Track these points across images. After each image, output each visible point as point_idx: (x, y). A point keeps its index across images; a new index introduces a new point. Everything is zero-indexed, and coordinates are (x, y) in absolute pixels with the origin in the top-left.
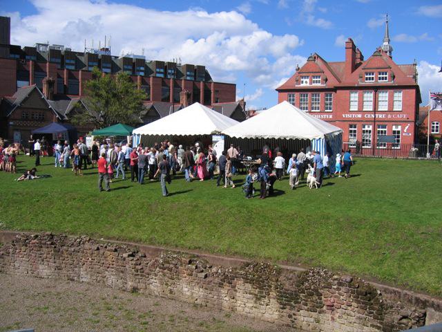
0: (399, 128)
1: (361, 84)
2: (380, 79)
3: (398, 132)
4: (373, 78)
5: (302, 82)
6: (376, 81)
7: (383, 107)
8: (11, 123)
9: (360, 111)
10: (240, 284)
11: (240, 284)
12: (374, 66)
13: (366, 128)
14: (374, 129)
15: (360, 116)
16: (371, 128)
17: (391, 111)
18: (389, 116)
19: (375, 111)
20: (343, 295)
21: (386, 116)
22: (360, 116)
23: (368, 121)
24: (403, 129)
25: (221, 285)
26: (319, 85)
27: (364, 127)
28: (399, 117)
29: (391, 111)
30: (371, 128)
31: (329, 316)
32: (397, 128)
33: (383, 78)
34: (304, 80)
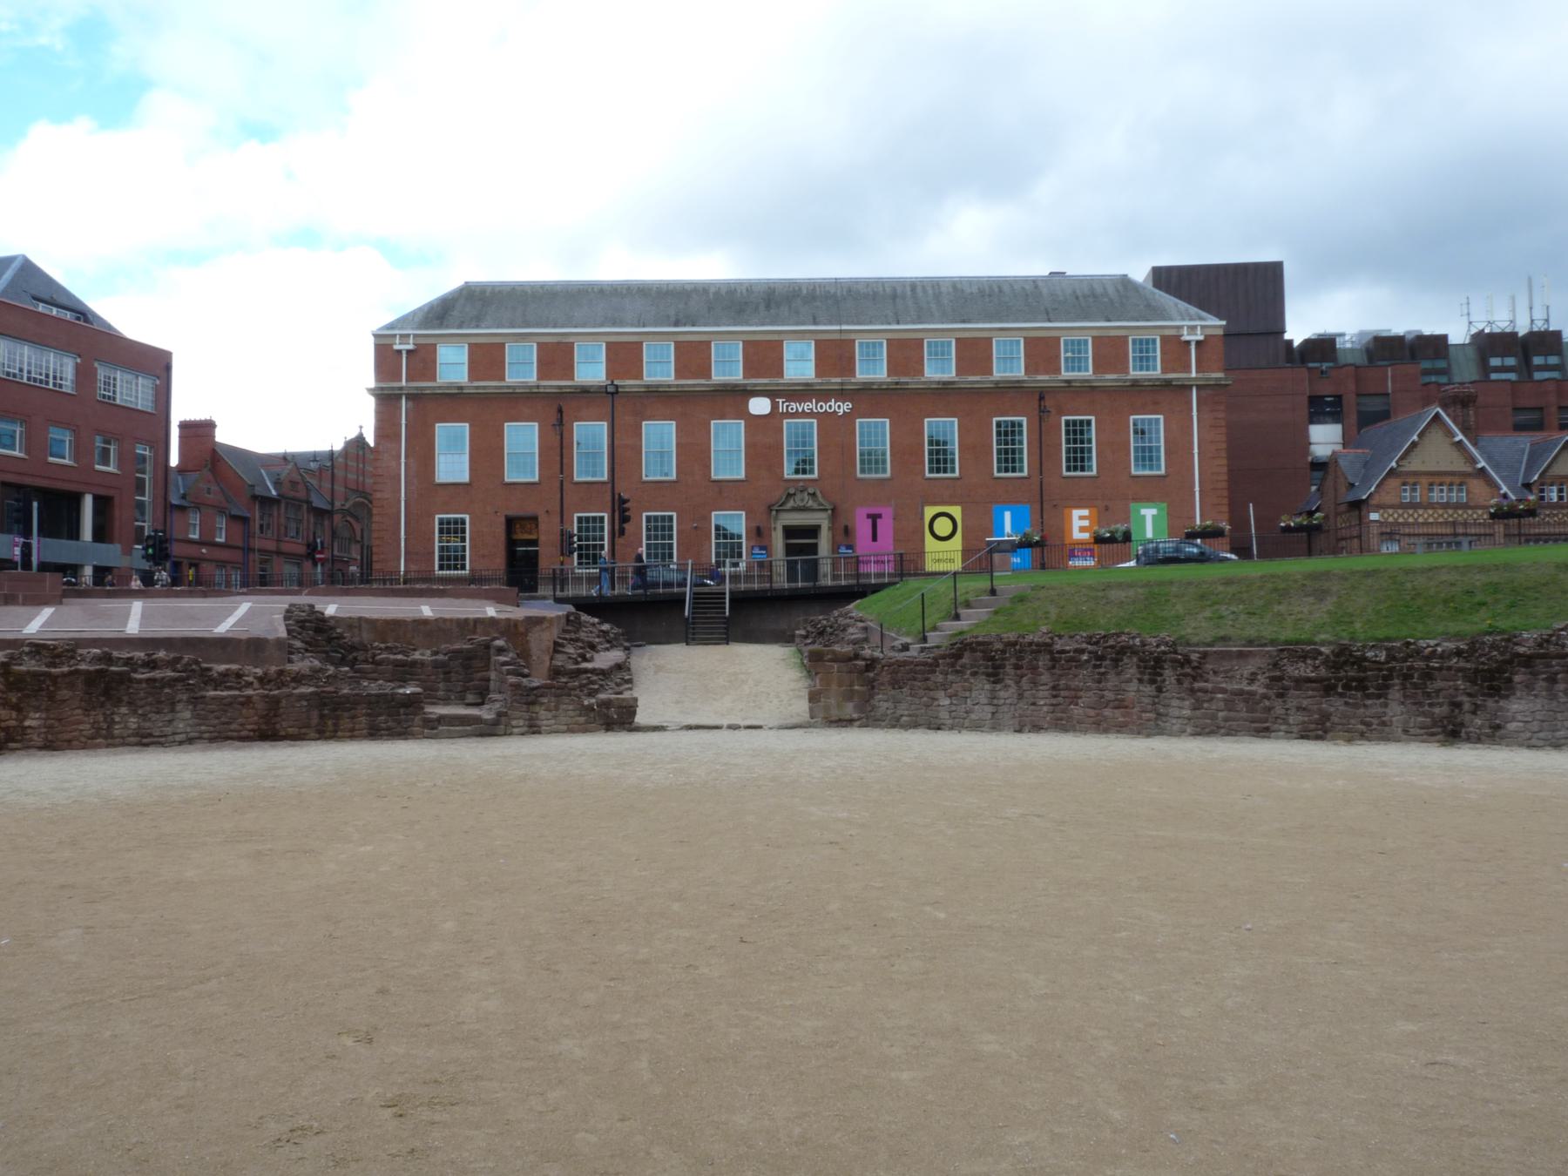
8: (1374, 516)
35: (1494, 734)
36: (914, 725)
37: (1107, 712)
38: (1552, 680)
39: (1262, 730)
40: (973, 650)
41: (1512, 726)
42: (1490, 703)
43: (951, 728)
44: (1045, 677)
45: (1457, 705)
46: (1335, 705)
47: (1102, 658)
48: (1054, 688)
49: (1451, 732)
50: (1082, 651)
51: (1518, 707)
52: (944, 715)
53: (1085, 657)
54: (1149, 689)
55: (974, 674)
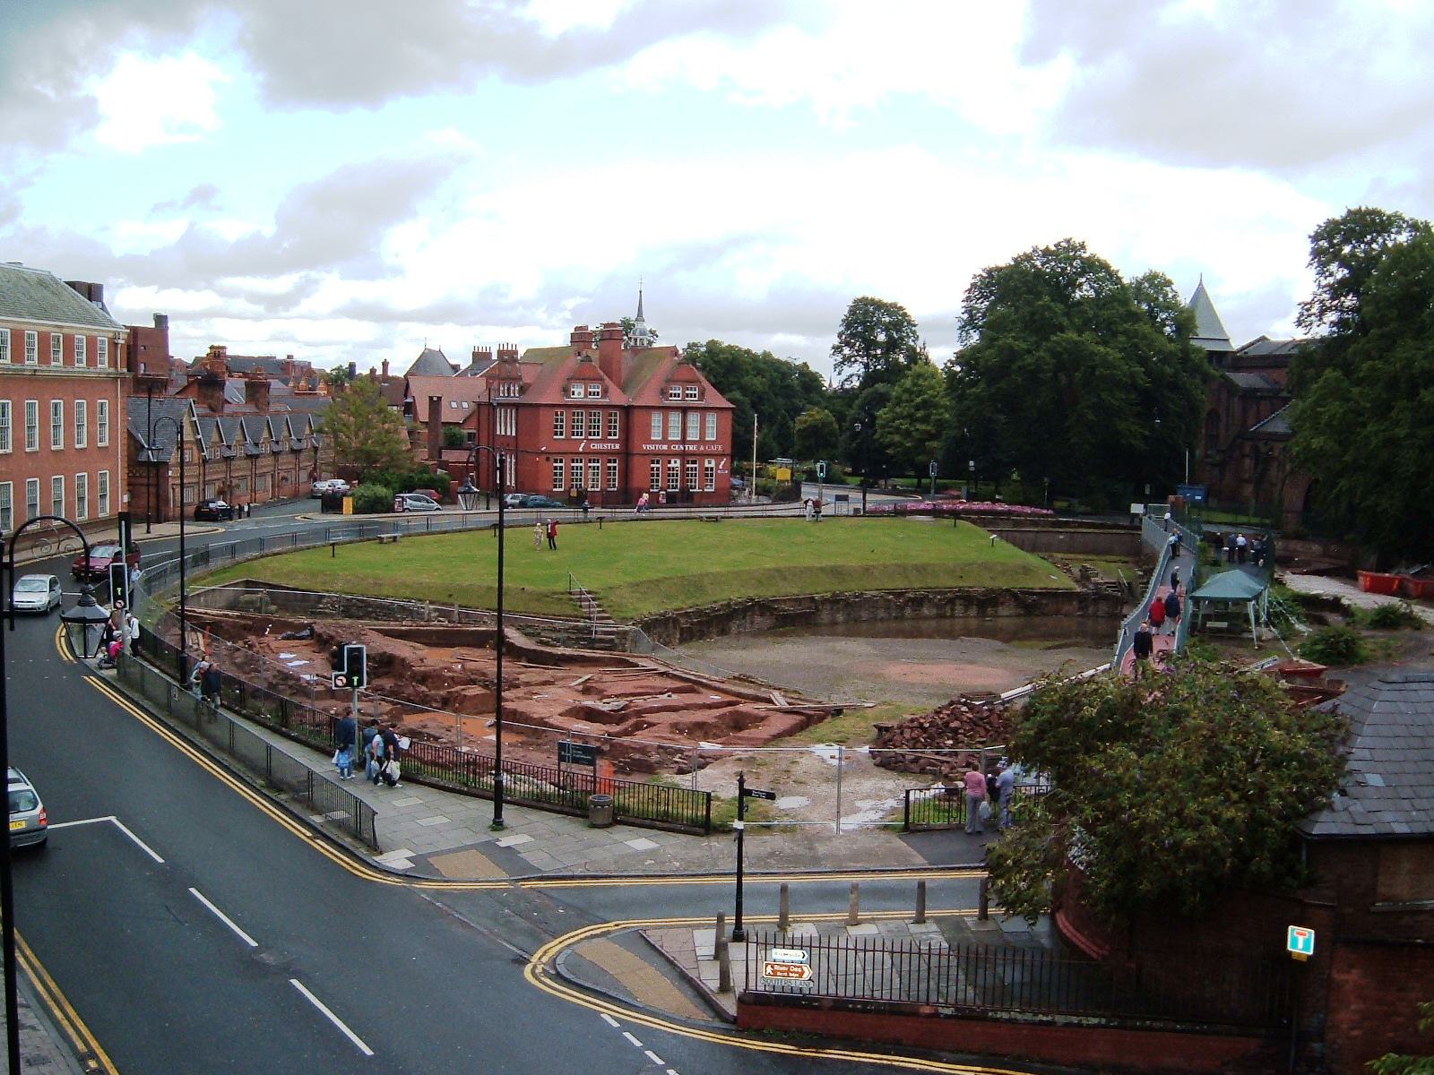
0: (713, 465)
1: (667, 403)
7: (693, 435)
9: (665, 441)
10: (958, 602)
11: (958, 602)
14: (683, 465)
15: (665, 447)
16: (678, 464)
17: (702, 441)
18: (702, 448)
19: (684, 441)
21: (698, 448)
22: (665, 447)
23: (675, 455)
24: (717, 465)
27: (670, 463)
28: (714, 448)
29: (702, 441)
32: (710, 463)
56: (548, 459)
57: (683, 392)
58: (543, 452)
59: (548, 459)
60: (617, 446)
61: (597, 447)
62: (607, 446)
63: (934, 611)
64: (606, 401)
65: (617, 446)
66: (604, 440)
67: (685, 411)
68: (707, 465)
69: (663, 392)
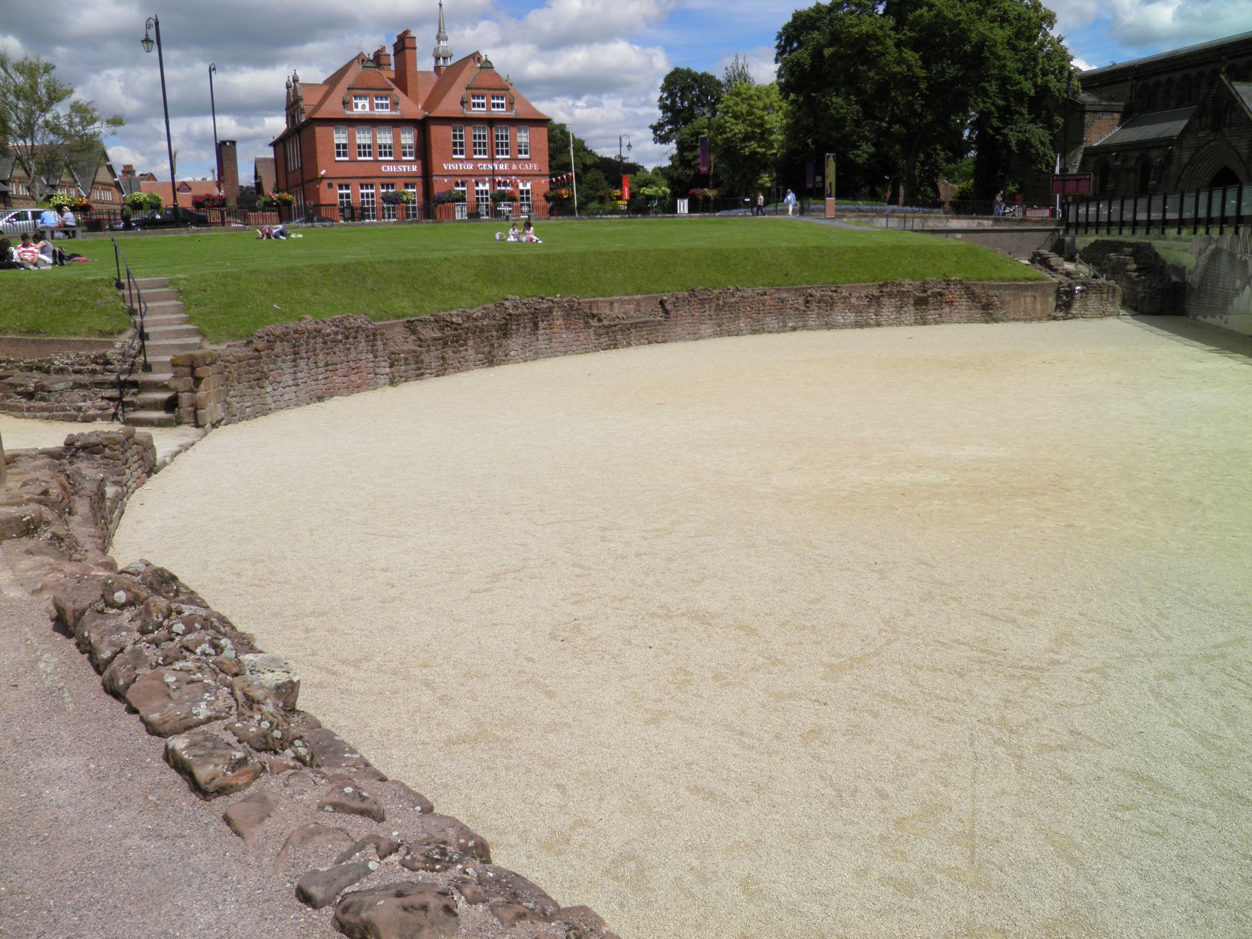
2: (494, 105)
3: (528, 192)
4: (483, 105)
5: (356, 106)
6: (488, 110)
10: (885, 300)
11: (885, 300)
12: (483, 84)
13: (481, 187)
14: (493, 187)
15: (470, 167)
16: (487, 187)
18: (514, 167)
20: (955, 293)
21: (510, 167)
22: (470, 167)
25: (869, 306)
26: (386, 113)
28: (528, 167)
30: (487, 187)
31: (947, 310)
32: (525, 185)
33: (498, 106)
34: (360, 103)
35: (506, 359)
36: (255, 415)
37: (353, 378)
38: (525, 327)
39: (420, 376)
40: (282, 341)
41: (513, 353)
42: (504, 342)
43: (277, 409)
44: (321, 357)
45: (492, 345)
46: (449, 353)
47: (347, 338)
48: (327, 365)
49: (490, 361)
50: (336, 333)
51: (514, 343)
52: (269, 400)
53: (340, 337)
54: (370, 356)
55: (284, 361)
56: (330, 186)
57: (488, 102)
58: (323, 178)
59: (330, 186)
60: (414, 168)
61: (391, 169)
62: (403, 168)
63: (851, 317)
64: (396, 114)
65: (414, 168)
66: (397, 161)
67: (491, 122)
68: (521, 187)
69: (462, 103)
